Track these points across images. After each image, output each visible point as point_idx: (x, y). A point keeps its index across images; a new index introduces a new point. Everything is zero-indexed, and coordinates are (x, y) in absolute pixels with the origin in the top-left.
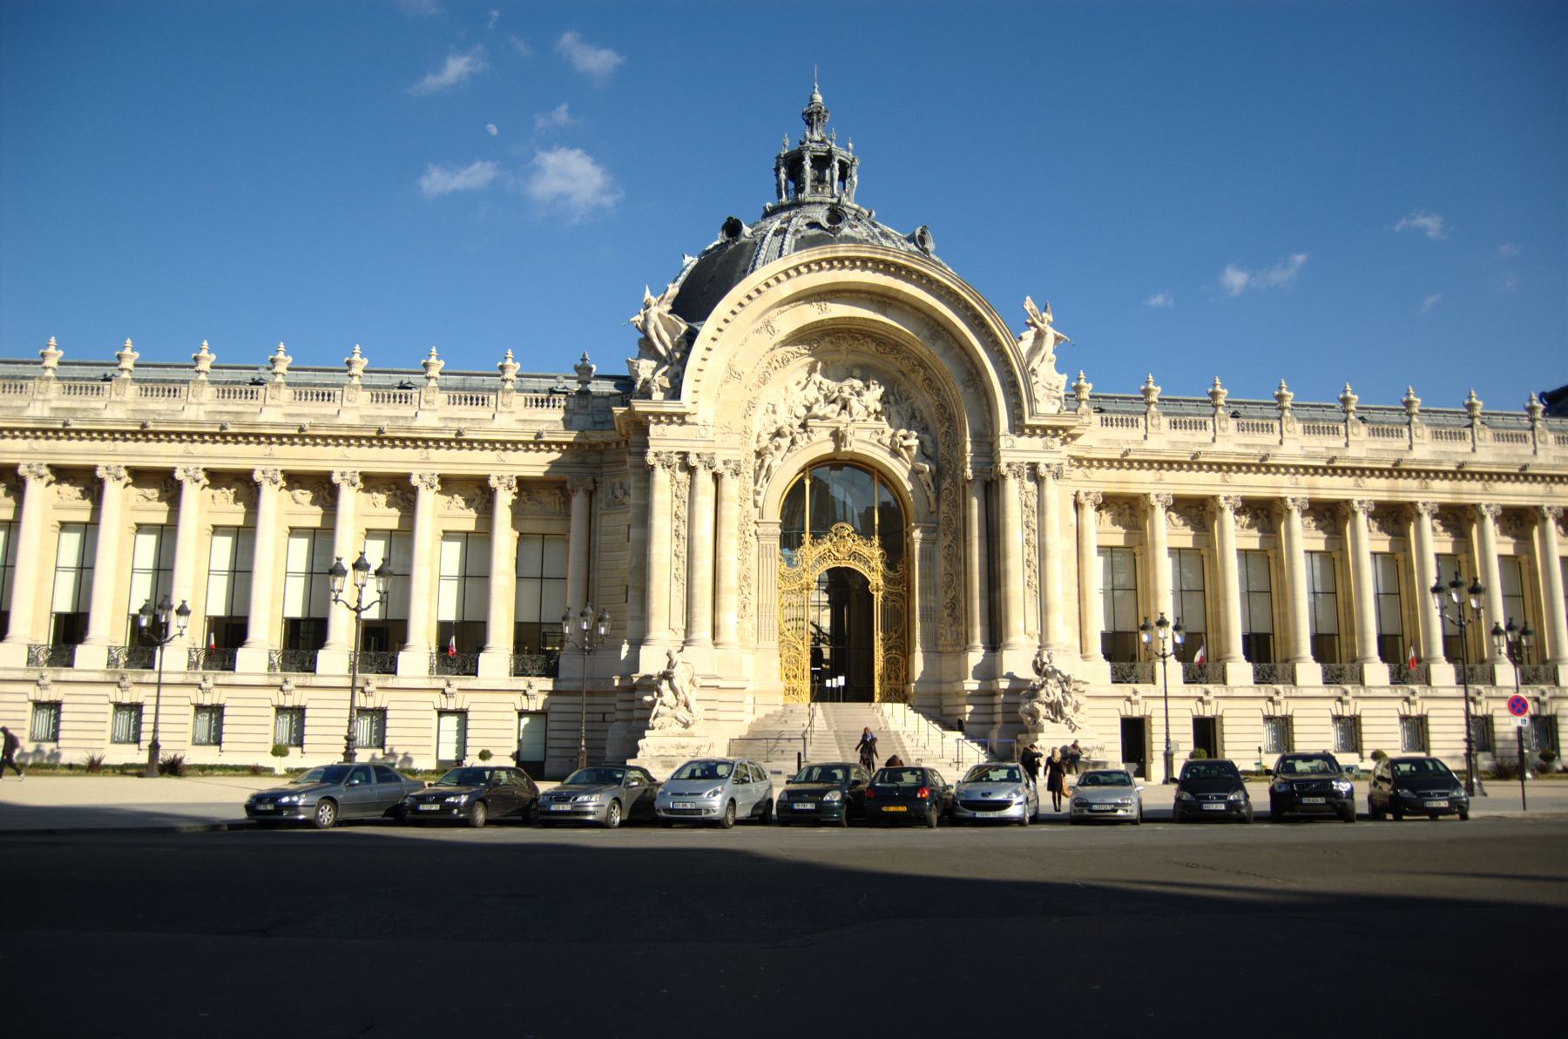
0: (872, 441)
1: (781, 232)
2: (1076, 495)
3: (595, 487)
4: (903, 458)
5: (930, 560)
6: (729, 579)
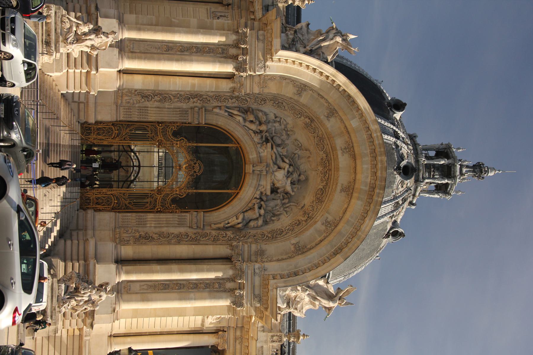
2: (224, 331)
5: (179, 224)
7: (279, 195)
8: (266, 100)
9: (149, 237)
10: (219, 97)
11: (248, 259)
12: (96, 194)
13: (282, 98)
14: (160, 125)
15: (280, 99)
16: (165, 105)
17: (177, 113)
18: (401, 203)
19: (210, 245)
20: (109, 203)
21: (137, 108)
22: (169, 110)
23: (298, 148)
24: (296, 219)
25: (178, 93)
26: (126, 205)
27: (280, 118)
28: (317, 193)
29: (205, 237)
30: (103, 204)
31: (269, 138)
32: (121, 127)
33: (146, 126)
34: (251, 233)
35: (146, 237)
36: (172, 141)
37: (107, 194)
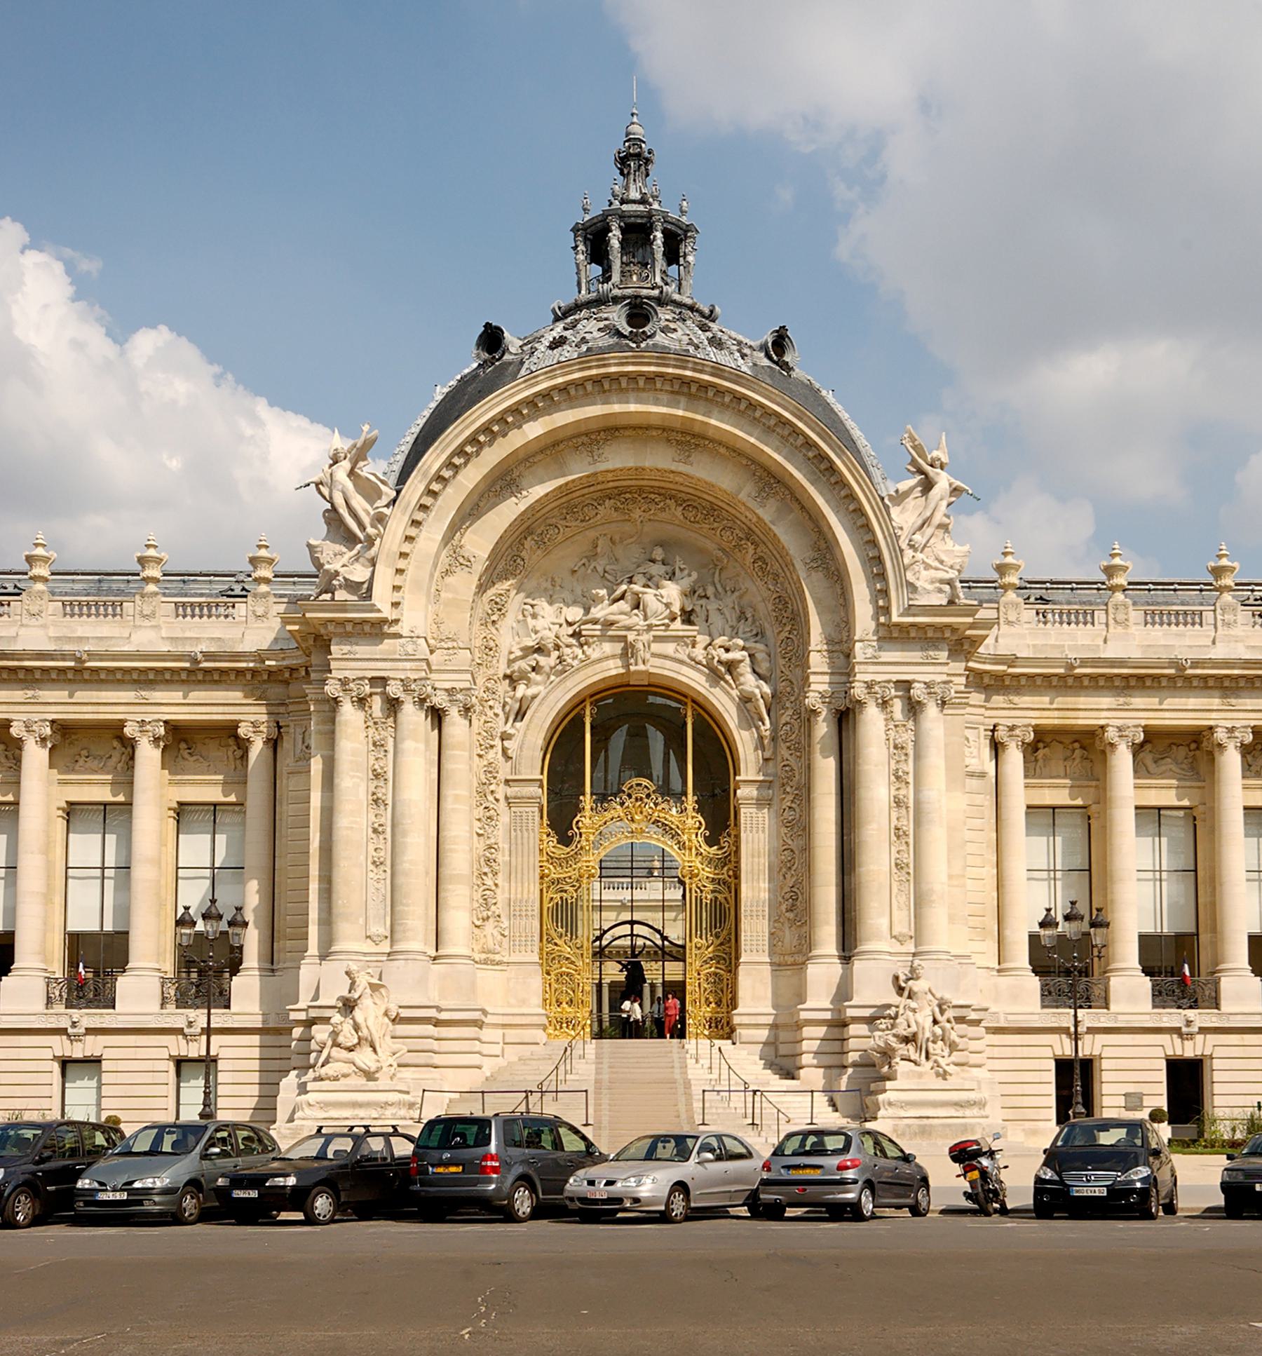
0: (678, 656)
1: (557, 343)
3: (279, 732)
4: (727, 682)
6: (460, 860)
7: (698, 609)
11: (841, 674)
17: (519, 836)
18: (709, 334)
19: (809, 760)
26: (721, 944)
28: (692, 519)
29: (792, 770)
31: (570, 630)
36: (582, 848)
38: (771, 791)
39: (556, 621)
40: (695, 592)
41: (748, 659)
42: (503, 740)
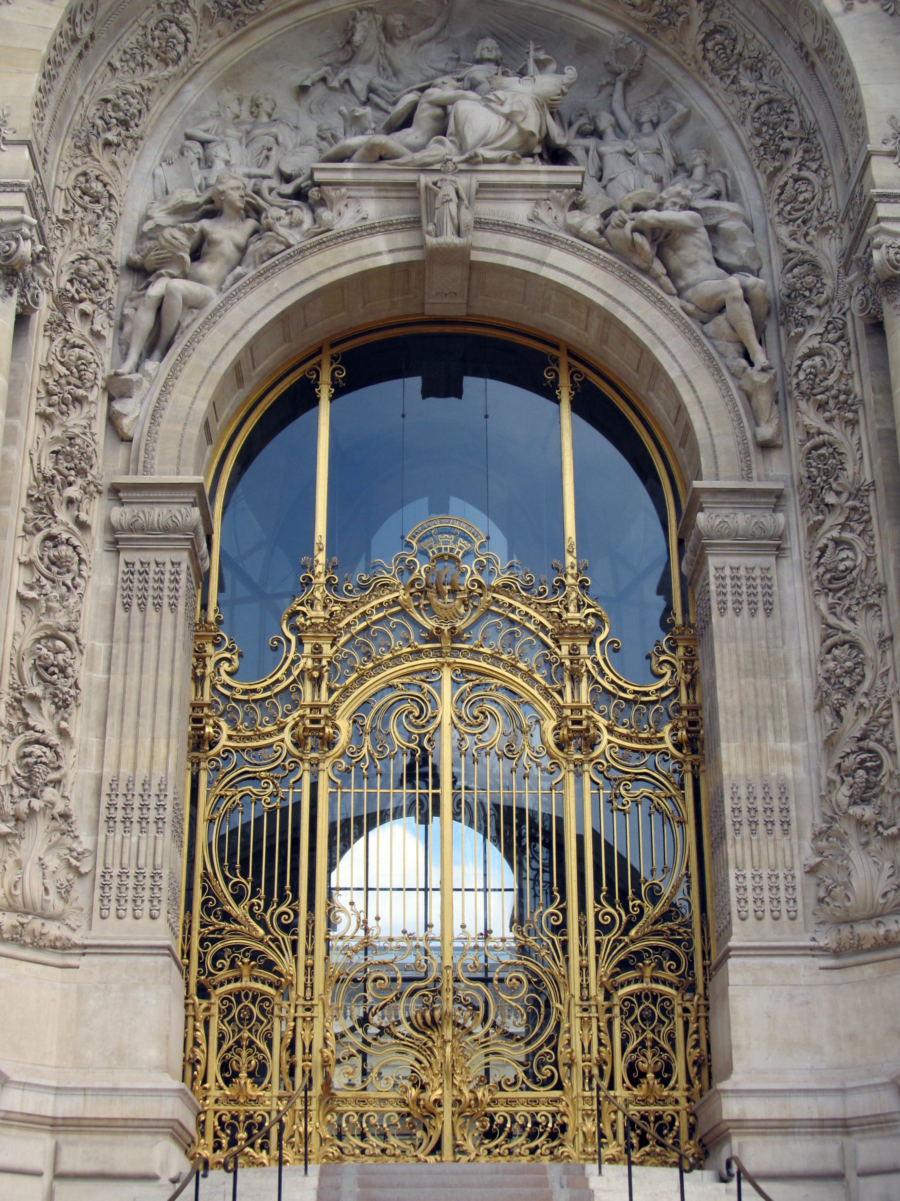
5: (768, 612)
7: (578, 153)
8: (85, 174)
9: (861, 749)
10: (57, 390)
12: (611, 1086)
13: (82, 98)
14: (209, 730)
15: (81, 111)
16: (90, 680)
20: (657, 1012)
21: (102, 838)
22: (121, 662)
23: (342, 76)
24: (700, 55)
25: (22, 599)
27: (188, 143)
29: (836, 453)
30: (667, 1047)
31: (288, 189)
32: (219, 945)
33: (216, 808)
34: (793, 245)
35: (867, 770)
37: (610, 1023)
38: (781, 517)
39: (255, 171)
40: (570, 124)
41: (703, 234)
42: (111, 399)
